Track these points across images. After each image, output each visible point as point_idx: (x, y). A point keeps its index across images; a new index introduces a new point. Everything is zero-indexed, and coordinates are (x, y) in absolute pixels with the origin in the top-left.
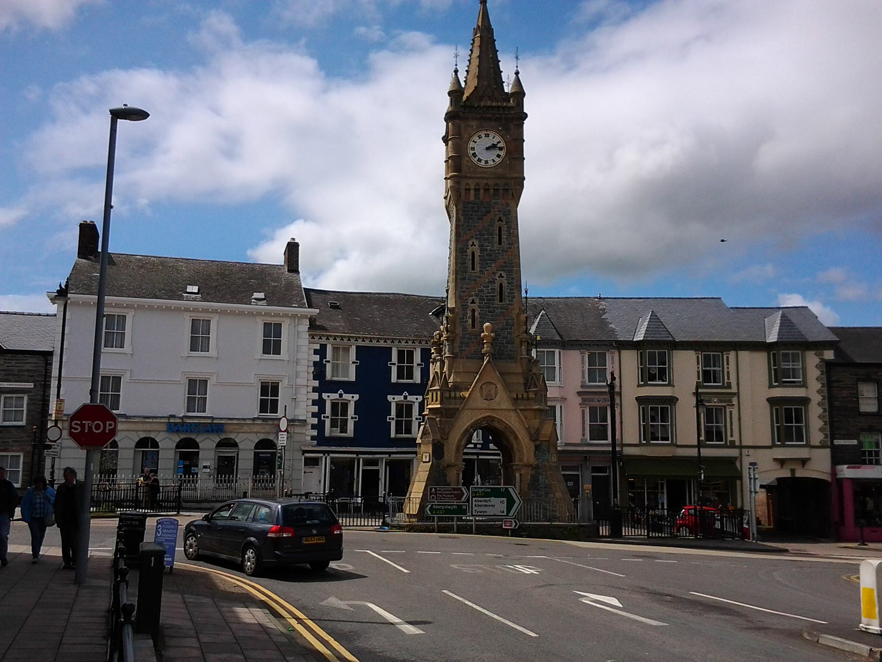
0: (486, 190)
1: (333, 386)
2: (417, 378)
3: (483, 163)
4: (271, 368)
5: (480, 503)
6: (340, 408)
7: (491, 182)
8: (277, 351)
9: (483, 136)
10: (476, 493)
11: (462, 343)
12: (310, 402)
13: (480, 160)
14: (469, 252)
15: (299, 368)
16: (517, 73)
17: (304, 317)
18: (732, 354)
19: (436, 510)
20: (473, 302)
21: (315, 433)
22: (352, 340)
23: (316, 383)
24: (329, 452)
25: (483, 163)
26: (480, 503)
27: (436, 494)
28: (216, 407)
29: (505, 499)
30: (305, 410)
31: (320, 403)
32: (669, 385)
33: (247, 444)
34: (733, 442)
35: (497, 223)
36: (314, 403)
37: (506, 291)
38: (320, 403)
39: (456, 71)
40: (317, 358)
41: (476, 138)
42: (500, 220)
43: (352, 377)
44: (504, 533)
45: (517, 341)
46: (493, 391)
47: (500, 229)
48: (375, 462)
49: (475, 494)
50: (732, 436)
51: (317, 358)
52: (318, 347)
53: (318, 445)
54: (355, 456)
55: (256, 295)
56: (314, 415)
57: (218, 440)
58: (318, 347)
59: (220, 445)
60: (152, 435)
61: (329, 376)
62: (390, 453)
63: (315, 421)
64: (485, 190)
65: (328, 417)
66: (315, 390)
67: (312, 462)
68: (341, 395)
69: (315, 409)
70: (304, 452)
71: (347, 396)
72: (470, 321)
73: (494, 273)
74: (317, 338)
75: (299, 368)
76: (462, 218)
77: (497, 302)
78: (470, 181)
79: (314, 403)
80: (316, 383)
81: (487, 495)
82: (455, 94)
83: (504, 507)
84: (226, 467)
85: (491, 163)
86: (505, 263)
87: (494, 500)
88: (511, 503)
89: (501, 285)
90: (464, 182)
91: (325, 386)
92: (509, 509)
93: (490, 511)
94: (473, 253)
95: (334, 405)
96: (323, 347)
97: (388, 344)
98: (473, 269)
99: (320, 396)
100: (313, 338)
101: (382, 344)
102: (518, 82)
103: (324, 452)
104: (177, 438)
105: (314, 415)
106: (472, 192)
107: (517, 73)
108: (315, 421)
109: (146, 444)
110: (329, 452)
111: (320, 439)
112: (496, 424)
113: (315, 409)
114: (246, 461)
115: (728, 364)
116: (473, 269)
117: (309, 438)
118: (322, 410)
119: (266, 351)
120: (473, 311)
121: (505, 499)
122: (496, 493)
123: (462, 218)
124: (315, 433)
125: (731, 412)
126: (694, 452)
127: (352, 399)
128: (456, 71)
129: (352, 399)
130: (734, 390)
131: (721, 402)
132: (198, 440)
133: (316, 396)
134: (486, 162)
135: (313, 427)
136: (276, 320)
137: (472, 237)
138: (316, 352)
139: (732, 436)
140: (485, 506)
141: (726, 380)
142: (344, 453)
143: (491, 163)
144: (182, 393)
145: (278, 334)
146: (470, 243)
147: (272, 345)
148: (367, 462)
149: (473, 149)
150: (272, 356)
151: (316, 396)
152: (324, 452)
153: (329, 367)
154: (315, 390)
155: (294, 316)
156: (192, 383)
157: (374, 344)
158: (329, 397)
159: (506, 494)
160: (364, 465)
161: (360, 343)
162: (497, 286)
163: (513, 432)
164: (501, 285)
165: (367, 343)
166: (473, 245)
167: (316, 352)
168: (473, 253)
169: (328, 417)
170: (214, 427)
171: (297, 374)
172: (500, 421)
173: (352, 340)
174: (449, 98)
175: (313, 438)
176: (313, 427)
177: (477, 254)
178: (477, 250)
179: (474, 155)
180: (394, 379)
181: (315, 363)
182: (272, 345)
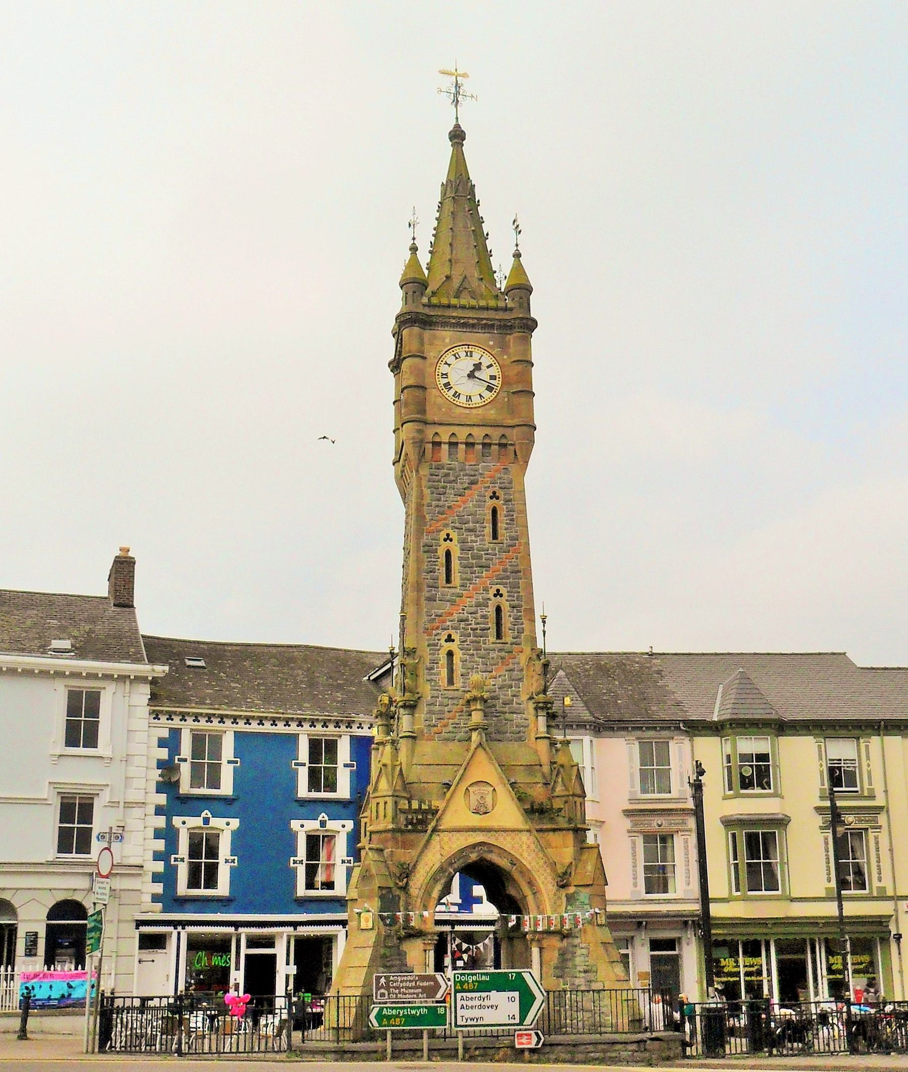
0: (470, 445)
2: (344, 790)
3: (463, 399)
4: (80, 772)
5: (470, 1003)
7: (478, 434)
8: (91, 741)
9: (462, 354)
10: (462, 983)
11: (430, 712)
12: (151, 833)
13: (457, 395)
14: (441, 553)
15: (132, 771)
16: (517, 255)
17: (141, 679)
18: (875, 740)
19: (389, 1018)
20: (449, 639)
21: (159, 888)
22: (228, 722)
23: (162, 799)
24: (184, 924)
25: (463, 399)
26: (470, 1003)
27: (388, 988)
29: (516, 994)
30: (140, 847)
31: (169, 835)
32: (775, 795)
34: (882, 889)
35: (491, 503)
36: (158, 834)
38: (169, 835)
39: (414, 249)
40: (164, 754)
41: (450, 358)
42: (494, 496)
43: (226, 788)
44: (518, 1055)
45: (531, 705)
46: (489, 799)
47: (494, 511)
48: (269, 942)
49: (461, 987)
50: (880, 880)
51: (164, 754)
52: (165, 734)
53: (165, 910)
54: (231, 930)
55: (56, 644)
56: (157, 856)
58: (165, 734)
61: (185, 788)
62: (295, 924)
63: (160, 867)
64: (468, 444)
65: (182, 860)
66: (159, 811)
67: (153, 942)
68: (206, 821)
69: (160, 845)
70: (140, 923)
71: (216, 822)
72: (444, 672)
73: (486, 590)
74: (163, 719)
75: (132, 771)
76: (427, 492)
77: (492, 638)
78: (440, 429)
79: (158, 834)
81: (483, 987)
82: (414, 284)
83: (515, 1008)
85: (476, 400)
86: (505, 570)
89: (498, 610)
90: (430, 432)
91: (179, 803)
92: (525, 1008)
93: (490, 1017)
94: (448, 554)
96: (176, 733)
97: (293, 728)
98: (448, 580)
99: (169, 822)
100: (157, 718)
101: (281, 728)
102: (518, 269)
103: (174, 924)
105: (157, 856)
106: (445, 447)
107: (517, 255)
108: (160, 867)
110: (184, 924)
112: (494, 858)
113: (160, 845)
115: (868, 758)
116: (448, 580)
117: (148, 898)
119: (72, 740)
120: (450, 654)
121: (516, 994)
122: (499, 984)
123: (427, 492)
124: (159, 888)
125: (876, 838)
126: (830, 909)
127: (226, 828)
128: (414, 249)
129: (226, 828)
130: (879, 802)
131: (860, 821)
133: (161, 822)
134: (469, 398)
135: (156, 878)
136: (93, 684)
137: (446, 525)
138: (162, 743)
139: (880, 880)
140: (480, 1007)
141: (866, 786)
142: (213, 924)
143: (476, 400)
145: (94, 710)
146: (443, 535)
147: (81, 729)
148: (253, 942)
149: (445, 375)
150: (81, 750)
151: (161, 822)
152: (174, 924)
153: (185, 770)
154: (159, 811)
155: (123, 678)
157: (267, 728)
160: (248, 947)
161: (241, 726)
162: (491, 611)
163: (524, 871)
164: (498, 610)
165: (254, 727)
166: (448, 538)
167: (162, 743)
168: (448, 554)
169: (182, 860)
172: (502, 851)
173: (228, 722)
174: (400, 293)
175: (155, 898)
176: (156, 878)
177: (456, 553)
179: (447, 385)
180: (303, 791)
181: (161, 764)
182: (81, 729)
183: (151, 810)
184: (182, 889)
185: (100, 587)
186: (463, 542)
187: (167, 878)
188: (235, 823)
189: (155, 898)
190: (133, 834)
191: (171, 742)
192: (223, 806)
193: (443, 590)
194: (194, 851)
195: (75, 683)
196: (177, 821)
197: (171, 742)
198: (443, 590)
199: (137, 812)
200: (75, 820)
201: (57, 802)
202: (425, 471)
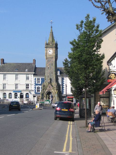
1: (37, 85)
4: (28, 82)
6: (38, 88)
8: (29, 79)
12: (34, 87)
17: (32, 74)
21: (35, 92)
23: (35, 84)
28: (20, 88)
30: (33, 88)
31: (35, 87)
33: (24, 94)
36: (34, 87)
37: (53, 73)
38: (35, 87)
40: (35, 80)
49: (45, 101)
51: (35, 80)
56: (34, 89)
57: (20, 93)
58: (35, 78)
59: (21, 94)
60: (11, 93)
63: (35, 90)
66: (34, 85)
69: (35, 88)
71: (40, 86)
75: (32, 82)
79: (34, 87)
80: (35, 84)
81: (47, 101)
83: (49, 102)
84: (22, 97)
87: (48, 102)
88: (50, 102)
89: (52, 72)
91: (36, 85)
95: (38, 87)
96: (36, 78)
103: (36, 95)
104: (14, 93)
105: (34, 89)
108: (35, 90)
109: (10, 94)
111: (36, 93)
113: (35, 88)
114: (24, 96)
118: (36, 88)
122: (48, 101)
127: (40, 86)
132: (17, 93)
133: (35, 86)
144: (14, 86)
147: (27, 78)
150: (28, 80)
151: (35, 86)
152: (36, 95)
154: (34, 85)
155: (31, 74)
156: (16, 84)
158: (37, 86)
159: (49, 101)
163: (52, 92)
164: (52, 72)
170: (19, 91)
171: (31, 83)
175: (34, 93)
178: (49, 67)
183: (34, 85)
184: (37, 92)
185: (32, 62)
186: (50, 66)
187: (35, 91)
188: (41, 86)
189: (34, 93)
190: (32, 87)
191: (35, 79)
192: (40, 85)
193: (48, 70)
194: (38, 89)
195: (18, 80)
196: (36, 86)
197: (35, 79)
198: (48, 70)
199: (32, 85)
200: (27, 85)
201: (26, 85)
202: (47, 60)
